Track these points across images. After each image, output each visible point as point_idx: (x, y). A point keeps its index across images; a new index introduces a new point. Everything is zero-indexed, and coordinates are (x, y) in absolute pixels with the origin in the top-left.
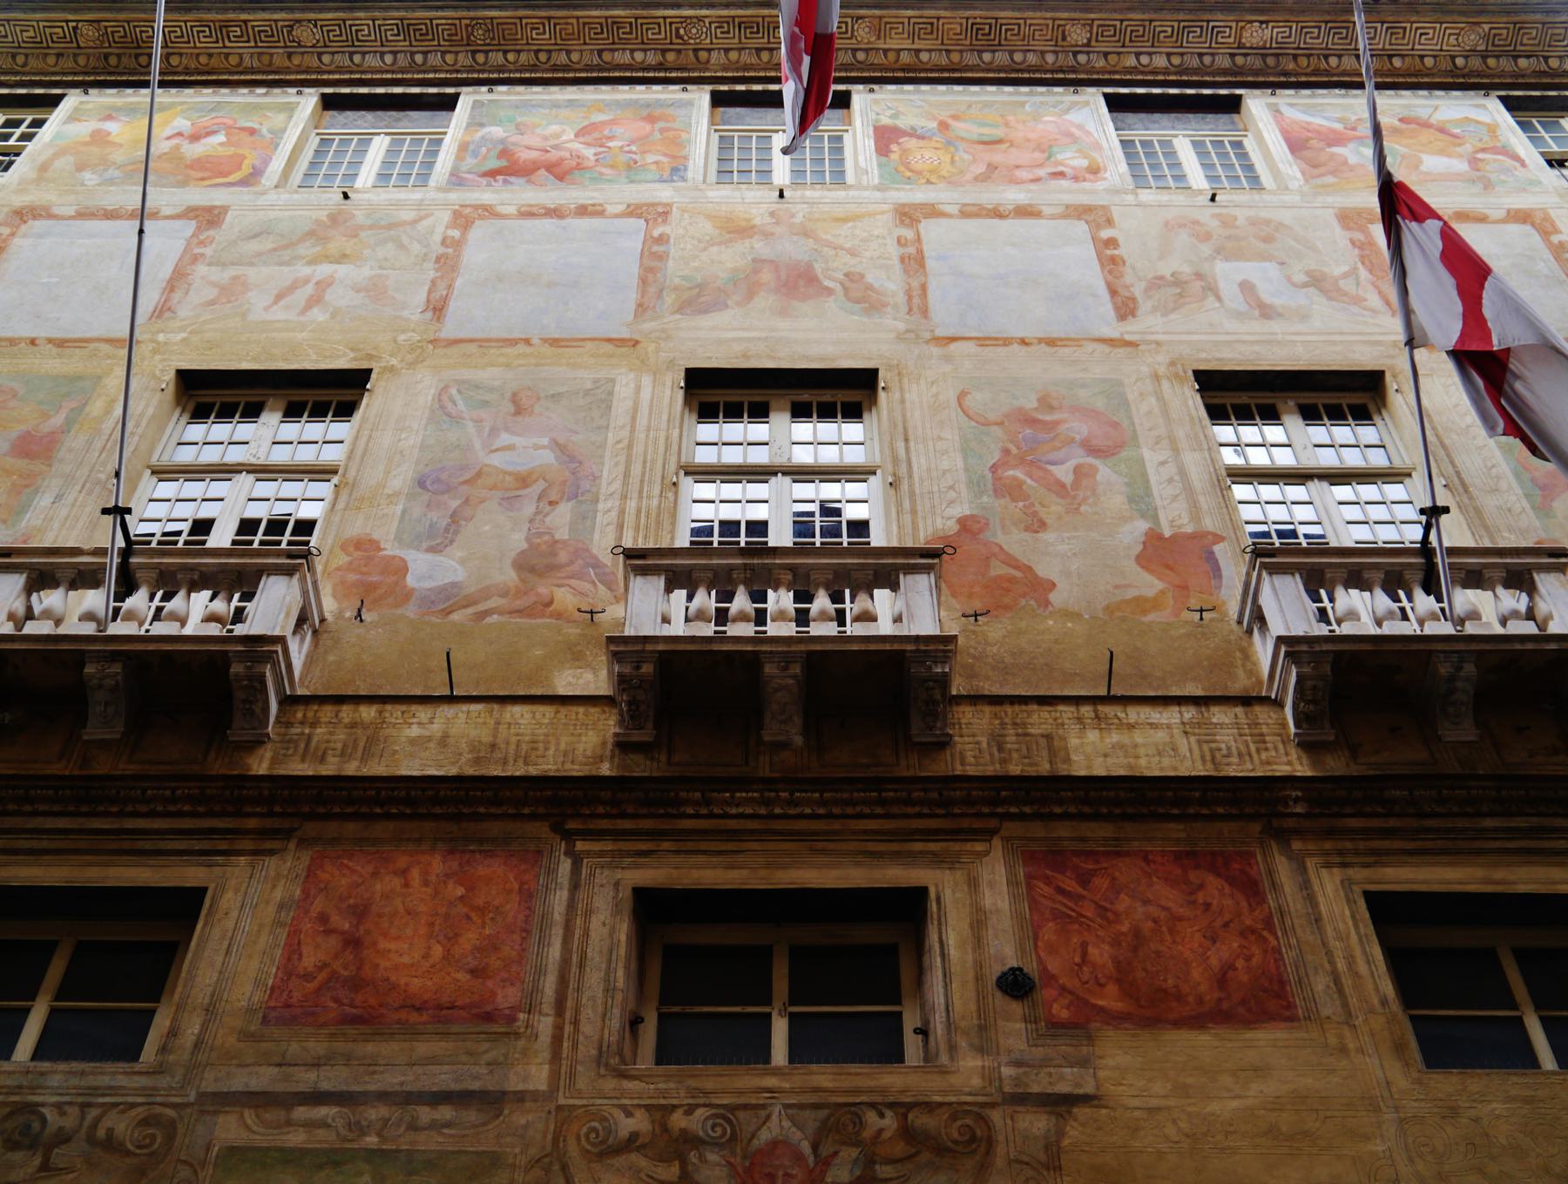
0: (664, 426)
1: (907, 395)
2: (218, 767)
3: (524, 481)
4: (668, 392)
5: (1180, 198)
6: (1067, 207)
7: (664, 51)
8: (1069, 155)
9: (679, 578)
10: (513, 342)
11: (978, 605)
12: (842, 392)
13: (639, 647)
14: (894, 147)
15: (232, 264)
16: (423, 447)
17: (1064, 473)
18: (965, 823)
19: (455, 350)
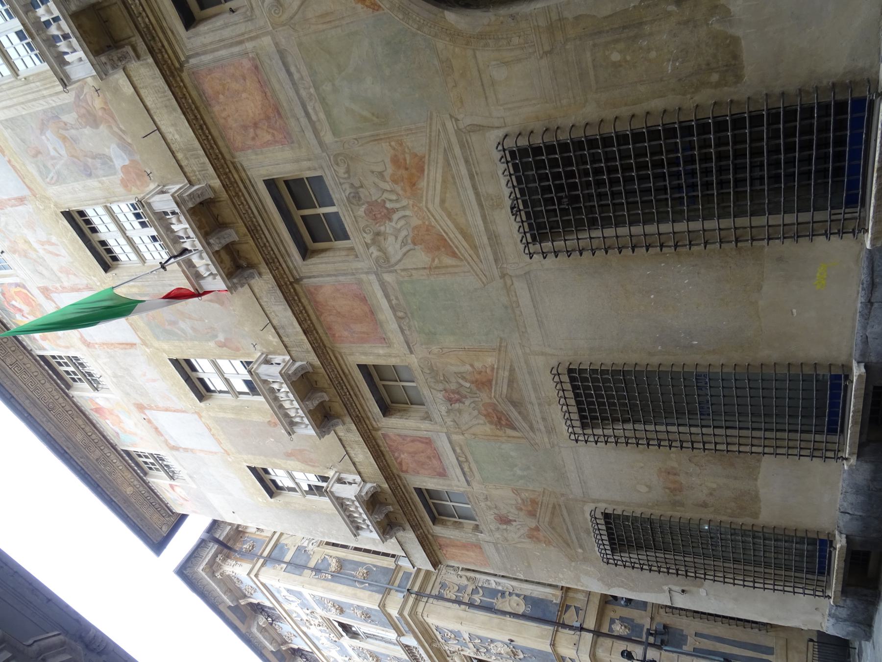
2: (224, 196)
3: (64, 139)
10: (13, 167)
19: (32, 187)
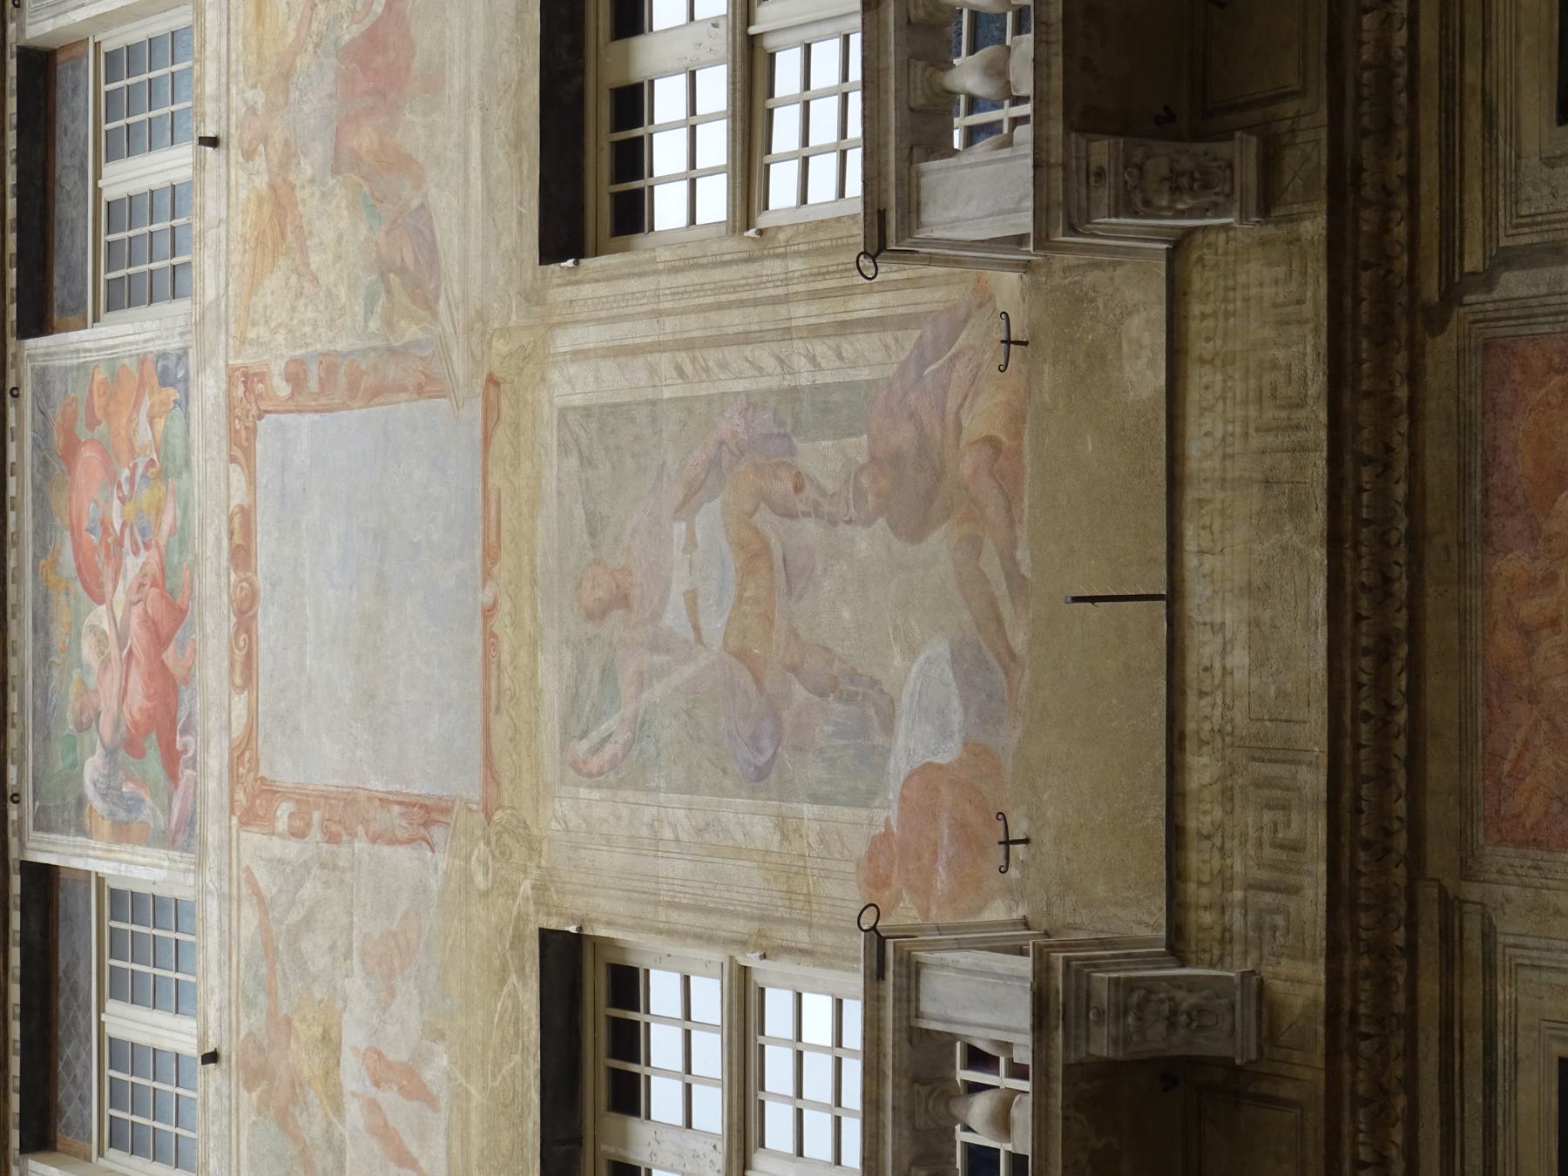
0: (648, 284)
2: (1310, 1071)
3: (754, 554)
4: (586, 290)
10: (490, 640)
13: (1057, 174)
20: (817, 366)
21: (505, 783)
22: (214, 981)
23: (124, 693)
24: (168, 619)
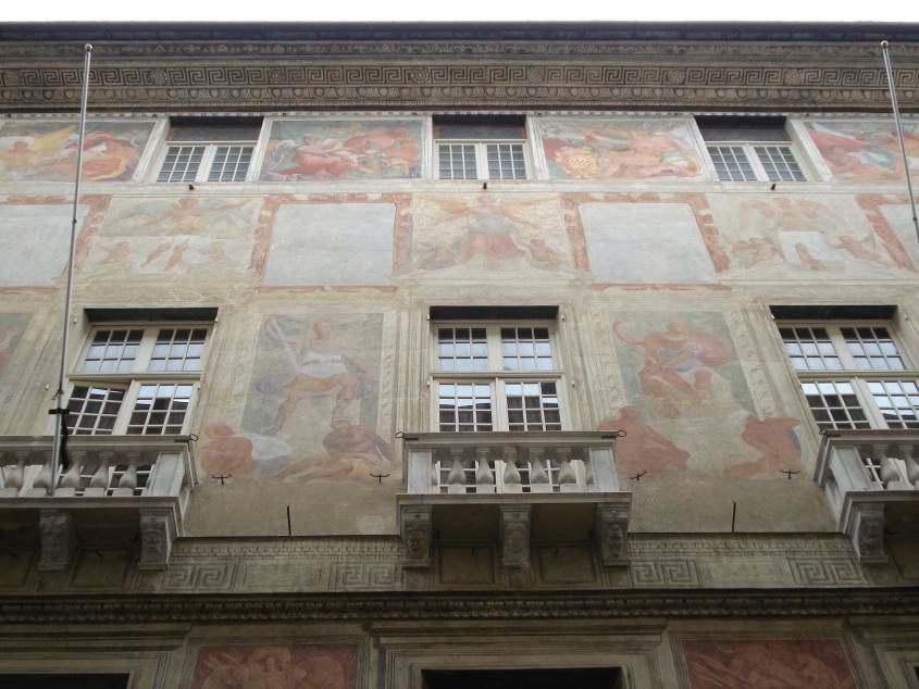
1: (579, 324)
2: (133, 586)
3: (327, 384)
4: (419, 323)
5: (751, 187)
6: (676, 193)
7: (400, 89)
8: (675, 158)
9: (442, 455)
10: (312, 289)
11: (640, 471)
12: (534, 321)
14: (558, 154)
15: (117, 234)
16: (257, 362)
17: (688, 377)
18: (643, 622)
20: (384, 403)
21: (267, 295)
22: (216, 188)
23: (313, 154)
24: (335, 171)
